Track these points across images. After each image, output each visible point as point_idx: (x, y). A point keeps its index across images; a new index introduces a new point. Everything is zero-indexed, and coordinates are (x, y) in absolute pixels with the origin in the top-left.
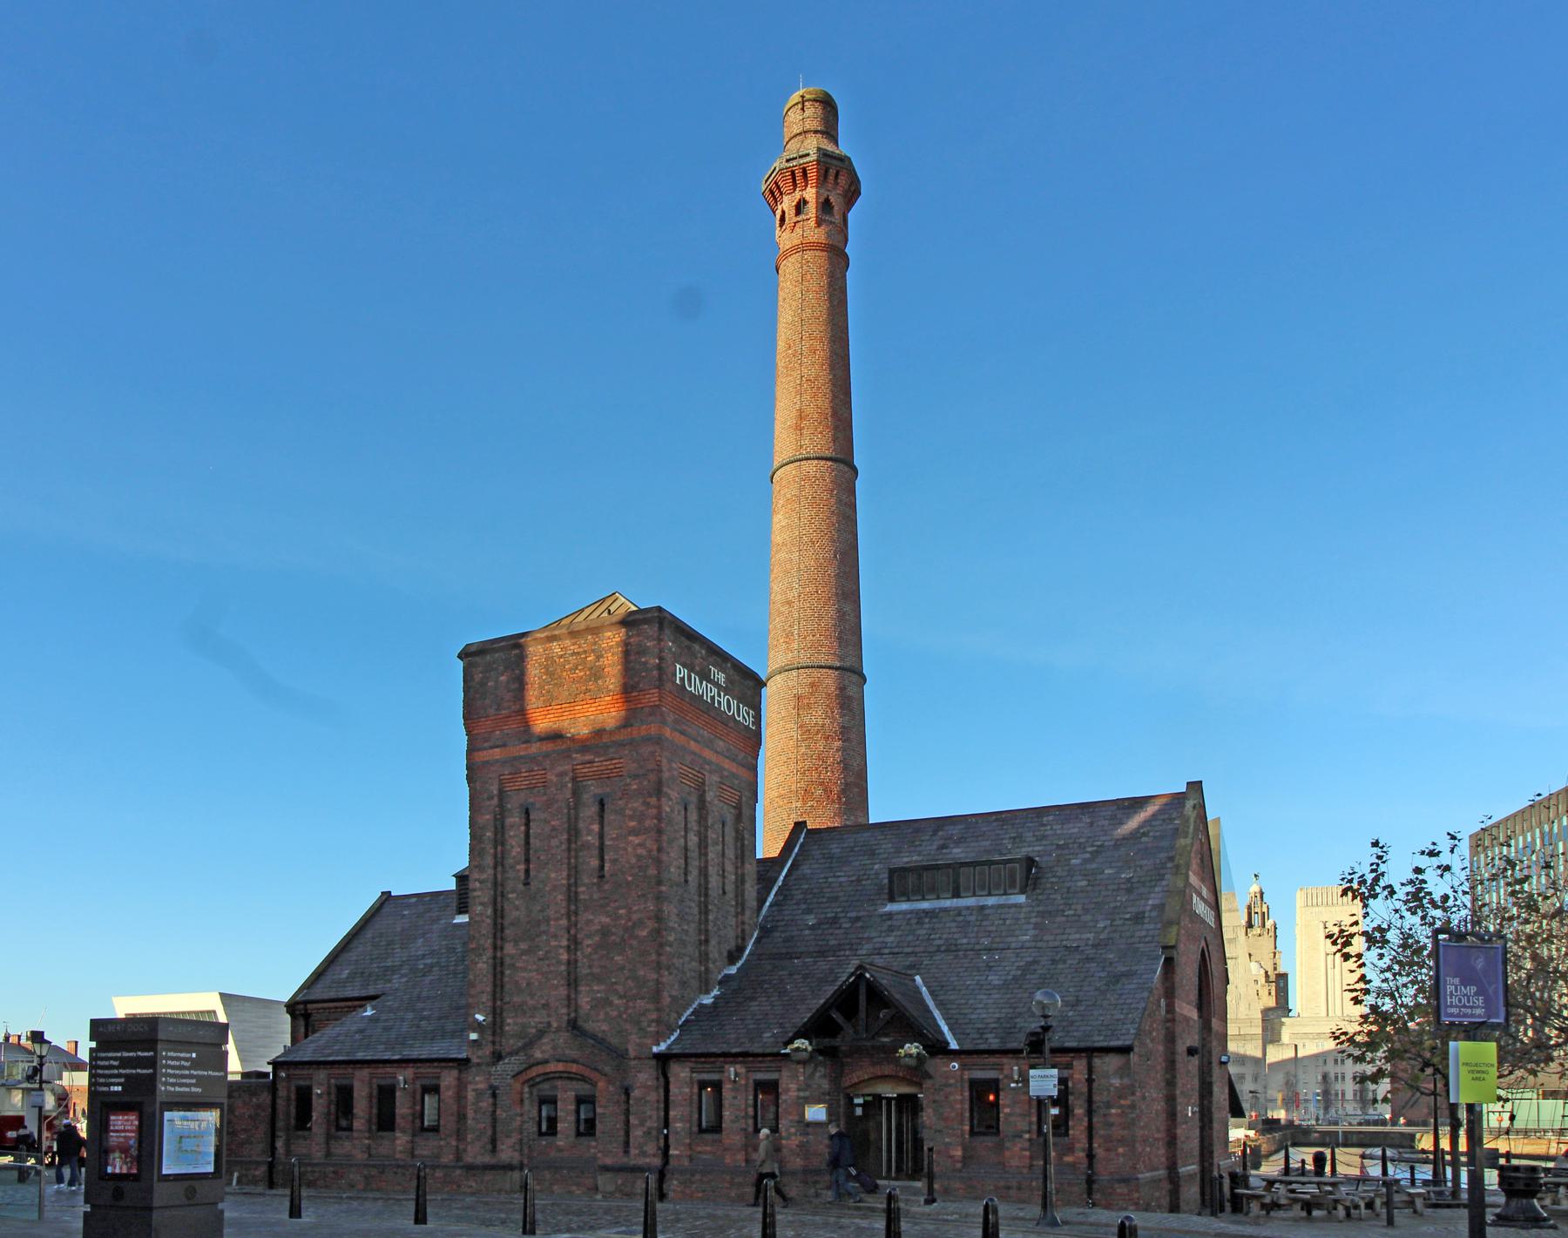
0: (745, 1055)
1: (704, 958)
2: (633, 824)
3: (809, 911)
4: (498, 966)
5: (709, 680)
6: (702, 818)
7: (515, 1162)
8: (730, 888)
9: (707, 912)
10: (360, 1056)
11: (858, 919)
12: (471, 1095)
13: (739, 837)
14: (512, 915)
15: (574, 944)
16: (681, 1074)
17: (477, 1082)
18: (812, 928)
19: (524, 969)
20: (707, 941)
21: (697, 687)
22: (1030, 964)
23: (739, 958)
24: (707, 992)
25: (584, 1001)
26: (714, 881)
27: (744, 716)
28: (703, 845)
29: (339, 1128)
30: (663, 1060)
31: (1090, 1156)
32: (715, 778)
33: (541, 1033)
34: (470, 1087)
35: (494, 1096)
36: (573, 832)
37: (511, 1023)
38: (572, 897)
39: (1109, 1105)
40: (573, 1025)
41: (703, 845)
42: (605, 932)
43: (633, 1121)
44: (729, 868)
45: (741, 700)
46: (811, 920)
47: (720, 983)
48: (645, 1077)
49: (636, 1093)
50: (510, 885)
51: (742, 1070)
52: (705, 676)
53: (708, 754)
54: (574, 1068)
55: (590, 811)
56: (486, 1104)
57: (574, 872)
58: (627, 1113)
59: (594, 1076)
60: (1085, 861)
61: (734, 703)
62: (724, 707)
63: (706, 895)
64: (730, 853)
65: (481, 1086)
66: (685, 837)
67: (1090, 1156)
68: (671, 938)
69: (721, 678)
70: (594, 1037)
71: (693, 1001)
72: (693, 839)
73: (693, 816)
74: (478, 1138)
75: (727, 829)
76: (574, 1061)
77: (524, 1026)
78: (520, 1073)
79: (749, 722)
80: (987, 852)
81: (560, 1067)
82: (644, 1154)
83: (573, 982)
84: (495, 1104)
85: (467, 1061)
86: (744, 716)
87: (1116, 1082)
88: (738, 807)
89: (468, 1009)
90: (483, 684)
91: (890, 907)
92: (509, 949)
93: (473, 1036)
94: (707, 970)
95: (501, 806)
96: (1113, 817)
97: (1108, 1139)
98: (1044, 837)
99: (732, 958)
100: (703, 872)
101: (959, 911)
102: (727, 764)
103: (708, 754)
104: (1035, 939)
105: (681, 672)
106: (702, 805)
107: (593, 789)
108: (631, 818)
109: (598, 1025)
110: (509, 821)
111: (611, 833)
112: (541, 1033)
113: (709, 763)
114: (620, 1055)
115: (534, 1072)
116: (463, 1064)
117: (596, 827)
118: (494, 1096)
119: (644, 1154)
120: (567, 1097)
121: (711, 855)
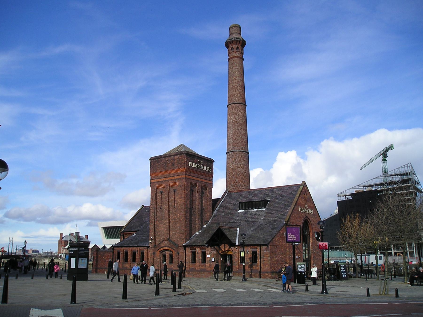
0: (200, 246)
3: (223, 212)
4: (155, 226)
7: (158, 269)
12: (149, 254)
14: (158, 215)
15: (169, 222)
16: (188, 250)
18: (223, 216)
25: (171, 233)
27: (209, 169)
29: (125, 261)
30: (185, 247)
31: (261, 267)
33: (163, 241)
36: (169, 198)
37: (158, 239)
38: (169, 212)
39: (264, 256)
40: (169, 239)
42: (175, 219)
46: (223, 214)
48: (181, 250)
49: (180, 254)
50: (158, 208)
51: (199, 249)
53: (198, 179)
54: (169, 248)
55: (172, 193)
57: (169, 206)
59: (172, 250)
60: (279, 200)
62: (205, 167)
67: (261, 267)
70: (173, 242)
76: (169, 247)
77: (160, 239)
79: (210, 170)
80: (261, 198)
81: (166, 248)
83: (169, 230)
85: (149, 246)
86: (209, 169)
87: (265, 251)
89: (149, 236)
91: (239, 211)
92: (158, 222)
93: (150, 241)
95: (156, 191)
97: (264, 264)
98: (273, 194)
102: (204, 180)
105: (190, 163)
107: (173, 188)
109: (174, 239)
110: (158, 195)
111: (176, 198)
112: (163, 241)
114: (177, 246)
115: (161, 249)
116: (149, 247)
117: (174, 197)
120: (168, 254)
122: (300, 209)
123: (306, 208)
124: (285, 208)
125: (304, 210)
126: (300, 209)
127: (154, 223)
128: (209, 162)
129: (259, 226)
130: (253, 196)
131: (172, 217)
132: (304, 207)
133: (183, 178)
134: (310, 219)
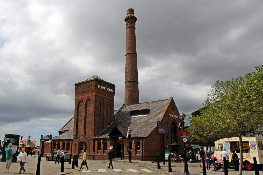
1: (103, 125)
2: (92, 107)
5: (104, 86)
6: (103, 105)
8: (109, 115)
9: (104, 118)
10: (61, 139)
11: (126, 118)
13: (111, 107)
14: (79, 119)
17: (74, 143)
18: (120, 120)
19: (80, 127)
20: (104, 123)
21: (102, 88)
22: (143, 125)
23: (110, 124)
24: (104, 130)
26: (105, 114)
28: (103, 109)
32: (106, 100)
34: (73, 143)
35: (75, 145)
41: (103, 109)
42: (89, 121)
43: (91, 148)
44: (109, 112)
45: (111, 88)
46: (121, 119)
47: (106, 129)
48: (92, 142)
49: (91, 144)
52: (104, 86)
53: (105, 96)
56: (74, 146)
58: (90, 147)
59: (86, 142)
61: (109, 89)
63: (104, 116)
64: (109, 110)
65: (74, 143)
66: (100, 108)
68: (97, 122)
69: (107, 86)
71: (102, 131)
72: (102, 108)
73: (102, 105)
74: (73, 151)
75: (109, 106)
77: (79, 135)
78: (79, 141)
79: (112, 91)
82: (92, 153)
84: (75, 146)
88: (111, 103)
90: (77, 88)
94: (104, 127)
96: (161, 103)
99: (109, 125)
100: (103, 113)
101: (138, 117)
102: (108, 97)
103: (105, 96)
104: (146, 121)
105: (99, 86)
106: (103, 104)
108: (92, 106)
111: (90, 108)
113: (105, 97)
118: (75, 145)
119: (92, 153)
121: (105, 110)
122: (169, 114)
123: (173, 114)
124: (159, 114)
125: (172, 116)
126: (169, 114)
127: (76, 124)
128: (112, 86)
129: (142, 126)
130: (140, 108)
131: (88, 120)
132: (172, 114)
133: (94, 95)
134: (176, 122)
